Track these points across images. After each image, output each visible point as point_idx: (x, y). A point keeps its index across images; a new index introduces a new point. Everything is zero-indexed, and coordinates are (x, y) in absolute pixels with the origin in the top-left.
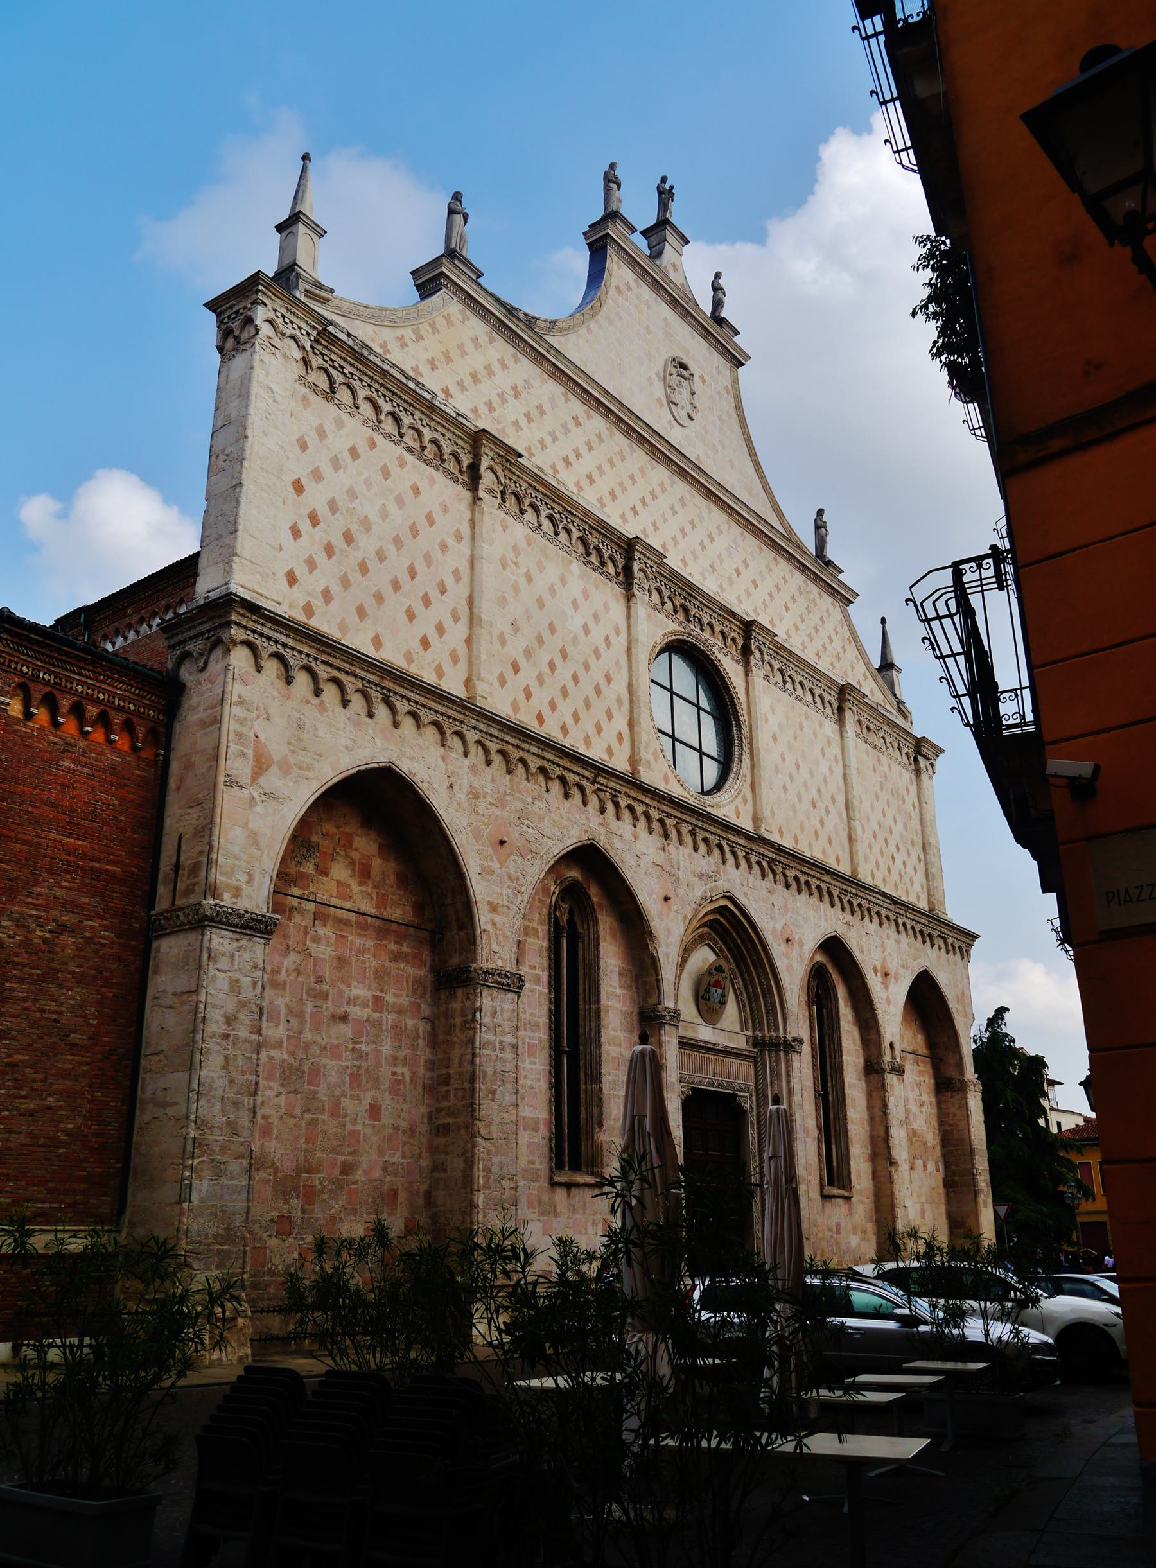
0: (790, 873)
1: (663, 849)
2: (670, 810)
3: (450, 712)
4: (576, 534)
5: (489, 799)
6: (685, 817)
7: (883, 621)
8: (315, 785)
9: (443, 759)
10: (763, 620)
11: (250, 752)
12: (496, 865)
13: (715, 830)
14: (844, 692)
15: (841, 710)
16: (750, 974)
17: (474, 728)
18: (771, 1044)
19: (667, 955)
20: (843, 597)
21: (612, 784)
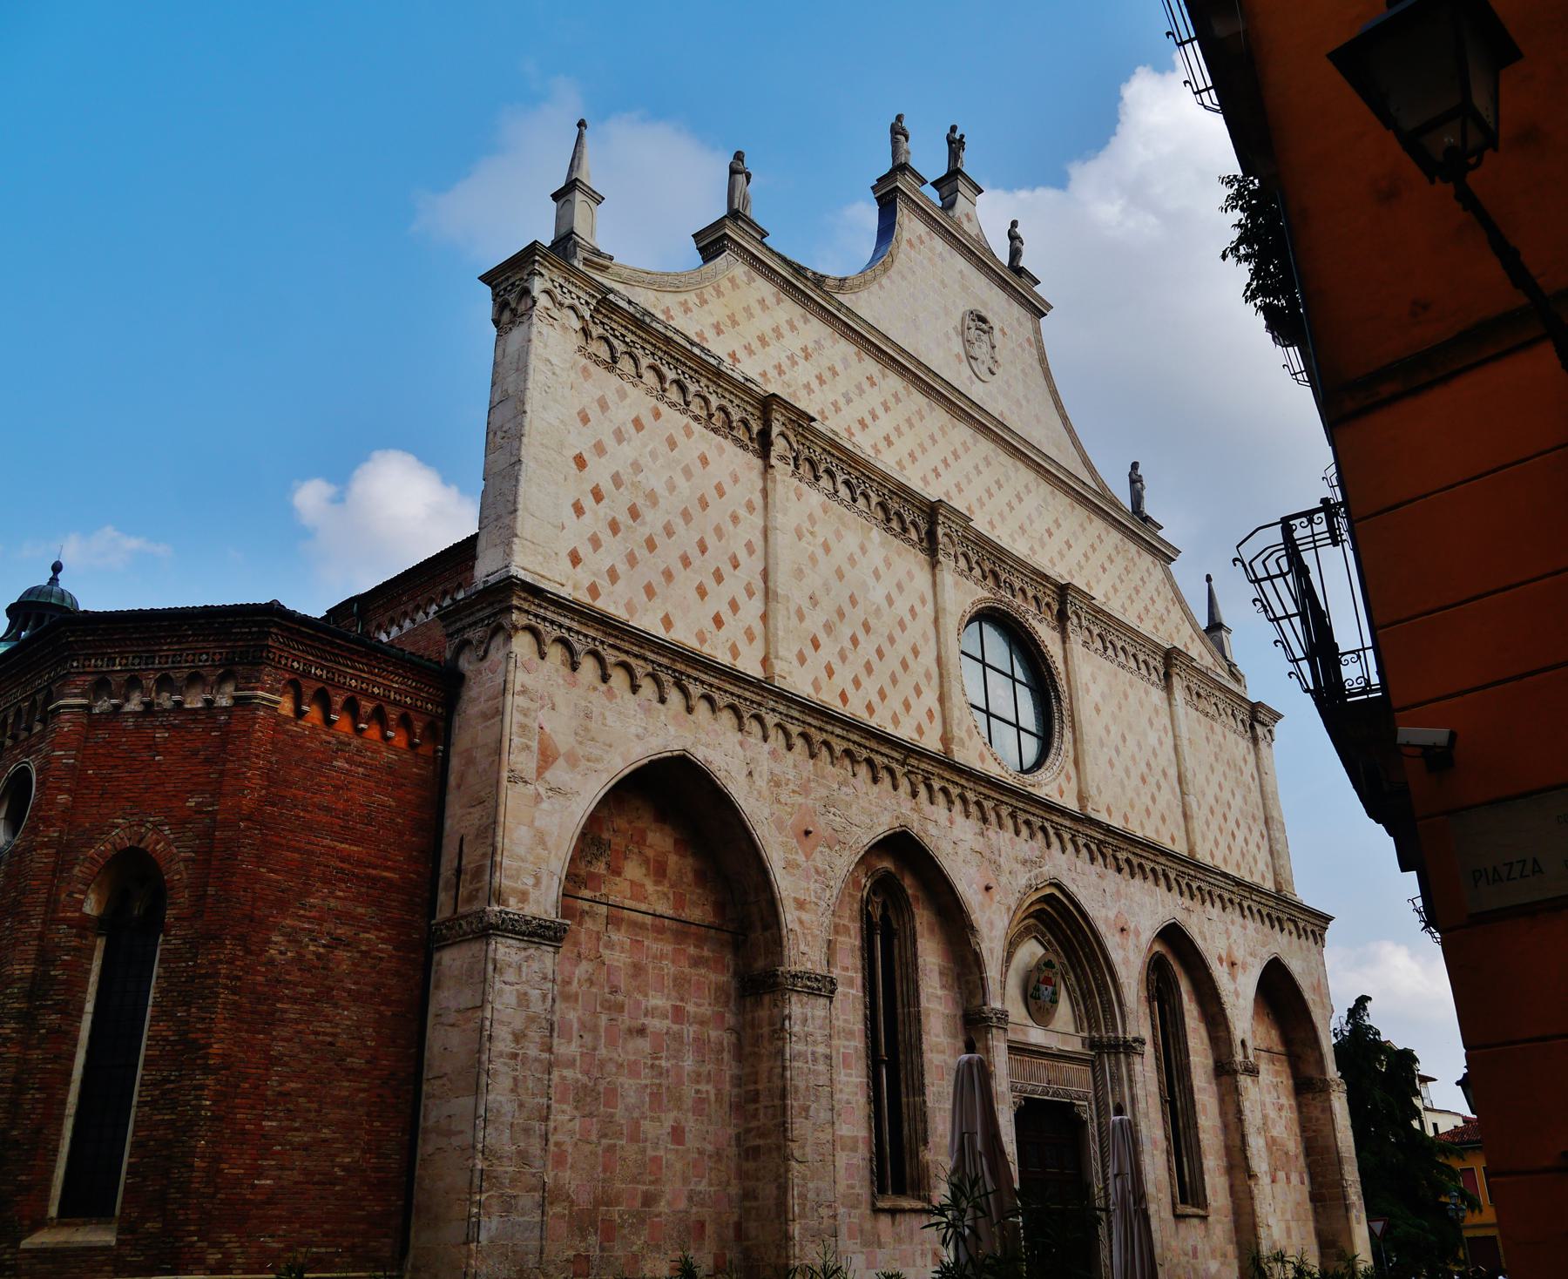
0: (1122, 856)
1: (982, 834)
2: (987, 792)
3: (747, 694)
4: (875, 499)
5: (791, 786)
6: (1005, 799)
7: (1209, 579)
8: (605, 778)
9: (741, 745)
10: (1079, 583)
11: (535, 745)
12: (801, 858)
13: (1037, 811)
14: (1171, 659)
15: (1167, 676)
16: (1083, 969)
17: (773, 710)
18: (1110, 1046)
19: (991, 951)
20: (1164, 554)
21: (923, 766)
